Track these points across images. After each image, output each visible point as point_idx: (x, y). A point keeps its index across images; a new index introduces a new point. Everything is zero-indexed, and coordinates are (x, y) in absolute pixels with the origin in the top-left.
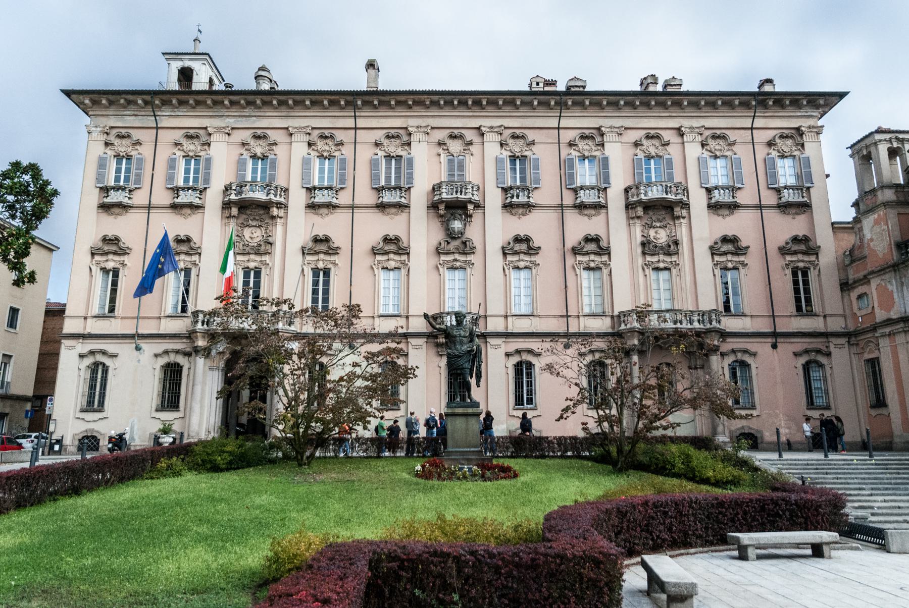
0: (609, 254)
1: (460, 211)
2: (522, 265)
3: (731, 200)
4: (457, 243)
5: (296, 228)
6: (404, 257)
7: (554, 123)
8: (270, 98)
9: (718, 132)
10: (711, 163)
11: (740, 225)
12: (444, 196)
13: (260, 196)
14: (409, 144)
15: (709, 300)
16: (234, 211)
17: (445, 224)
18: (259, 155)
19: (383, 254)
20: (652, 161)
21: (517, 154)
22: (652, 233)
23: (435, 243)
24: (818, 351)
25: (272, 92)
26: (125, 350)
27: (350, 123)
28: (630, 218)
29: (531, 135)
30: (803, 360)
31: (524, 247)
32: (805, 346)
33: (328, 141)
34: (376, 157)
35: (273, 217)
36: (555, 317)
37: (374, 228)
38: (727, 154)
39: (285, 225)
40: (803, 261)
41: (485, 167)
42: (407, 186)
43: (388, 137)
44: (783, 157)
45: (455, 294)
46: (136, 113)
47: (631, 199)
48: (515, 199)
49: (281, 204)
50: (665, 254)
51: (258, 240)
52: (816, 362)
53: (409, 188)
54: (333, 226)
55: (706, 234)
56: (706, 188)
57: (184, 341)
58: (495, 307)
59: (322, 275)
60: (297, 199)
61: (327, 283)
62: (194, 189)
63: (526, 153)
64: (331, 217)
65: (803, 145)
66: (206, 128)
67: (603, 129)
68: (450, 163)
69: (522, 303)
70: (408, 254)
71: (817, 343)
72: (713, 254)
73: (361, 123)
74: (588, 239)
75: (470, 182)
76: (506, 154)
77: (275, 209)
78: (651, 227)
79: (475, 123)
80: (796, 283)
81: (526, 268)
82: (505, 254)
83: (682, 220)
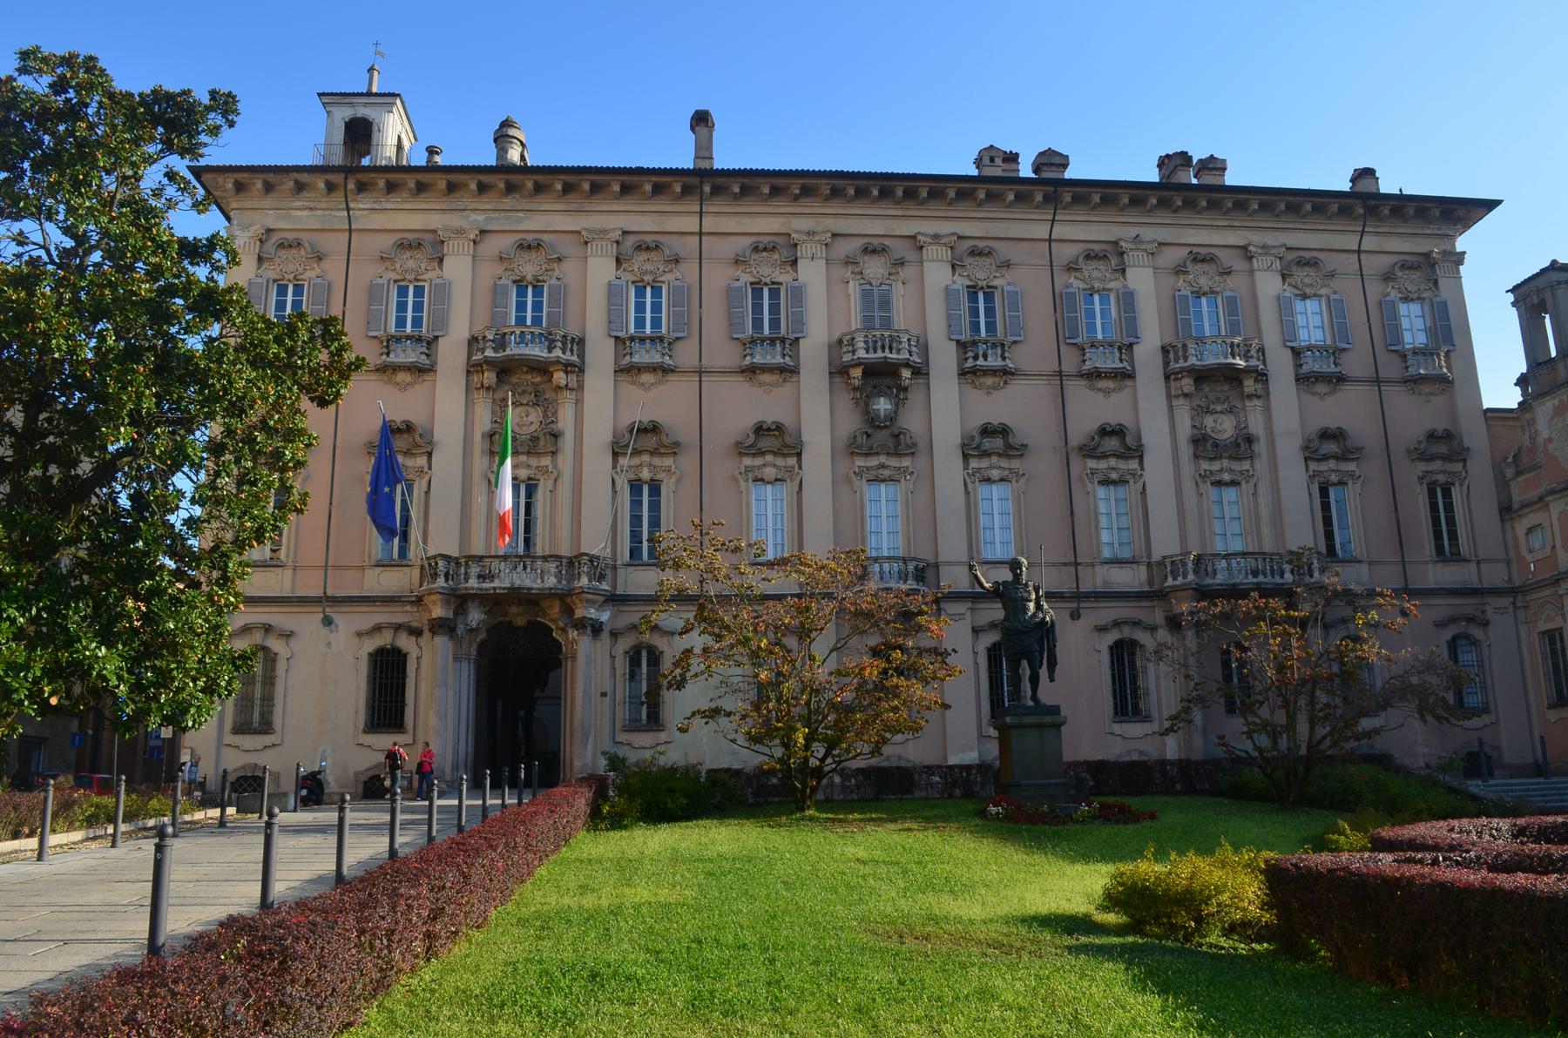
0: (1141, 458)
1: (889, 381)
2: (995, 474)
3: (1332, 369)
4: (882, 436)
5: (598, 408)
6: (792, 461)
7: (1041, 231)
8: (510, 180)
9: (1307, 255)
10: (1299, 305)
11: (1348, 409)
12: (861, 354)
13: (537, 351)
14: (794, 263)
15: (1302, 533)
16: (489, 377)
17: (862, 404)
18: (529, 278)
19: (754, 455)
20: (1204, 300)
21: (981, 283)
22: (1209, 421)
24: (1471, 620)
25: (525, 170)
26: (307, 623)
27: (691, 224)
28: (1169, 397)
29: (1003, 250)
30: (1447, 634)
31: (998, 442)
33: (652, 255)
34: (737, 284)
35: (559, 388)
37: (741, 407)
38: (1322, 292)
39: (579, 403)
40: (1444, 472)
41: (927, 302)
42: (792, 336)
43: (756, 249)
45: (885, 522)
46: (312, 205)
47: (1173, 365)
48: (981, 362)
49: (573, 365)
50: (1231, 458)
51: (532, 429)
52: (1467, 637)
53: (797, 339)
54: (667, 403)
55: (1295, 425)
56: (1292, 348)
57: (408, 608)
58: (952, 547)
59: (645, 491)
60: (601, 355)
61: (655, 507)
62: (419, 339)
63: (996, 282)
64: (662, 388)
65: (1436, 282)
66: (435, 231)
68: (866, 296)
69: (997, 540)
70: (799, 455)
71: (1468, 605)
72: (1306, 459)
73: (709, 224)
74: (1104, 432)
75: (906, 331)
76: (961, 282)
77: (562, 375)
78: (1209, 412)
79: (910, 228)
80: (1434, 507)
81: (1002, 480)
82: (966, 457)
83: (1256, 402)
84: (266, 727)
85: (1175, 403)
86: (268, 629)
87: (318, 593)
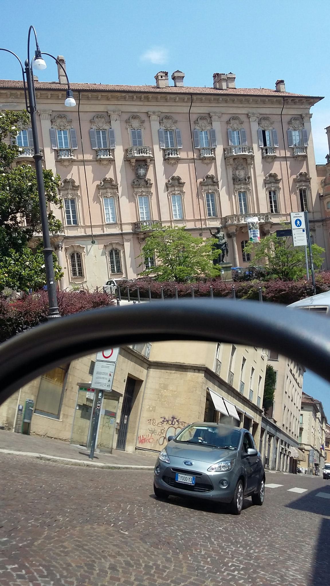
9: (265, 116)
12: (136, 155)
19: (103, 189)
23: (130, 181)
44: (295, 130)
48: (170, 156)
63: (173, 128)
67: (211, 114)
68: (133, 133)
72: (265, 183)
76: (163, 128)
79: (145, 109)
85: (227, 167)
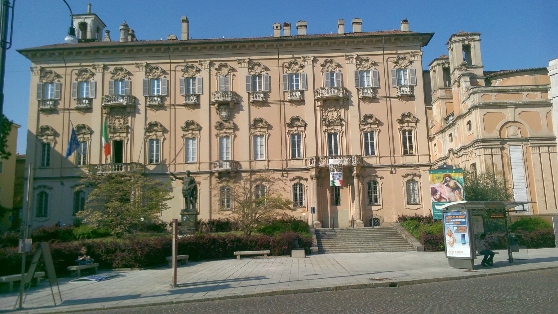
26: (56, 185)
29: (263, 63)
30: (406, 179)
32: (407, 172)
36: (276, 161)
48: (255, 99)
84: (45, 215)
86: (45, 187)
87: (59, 176)
